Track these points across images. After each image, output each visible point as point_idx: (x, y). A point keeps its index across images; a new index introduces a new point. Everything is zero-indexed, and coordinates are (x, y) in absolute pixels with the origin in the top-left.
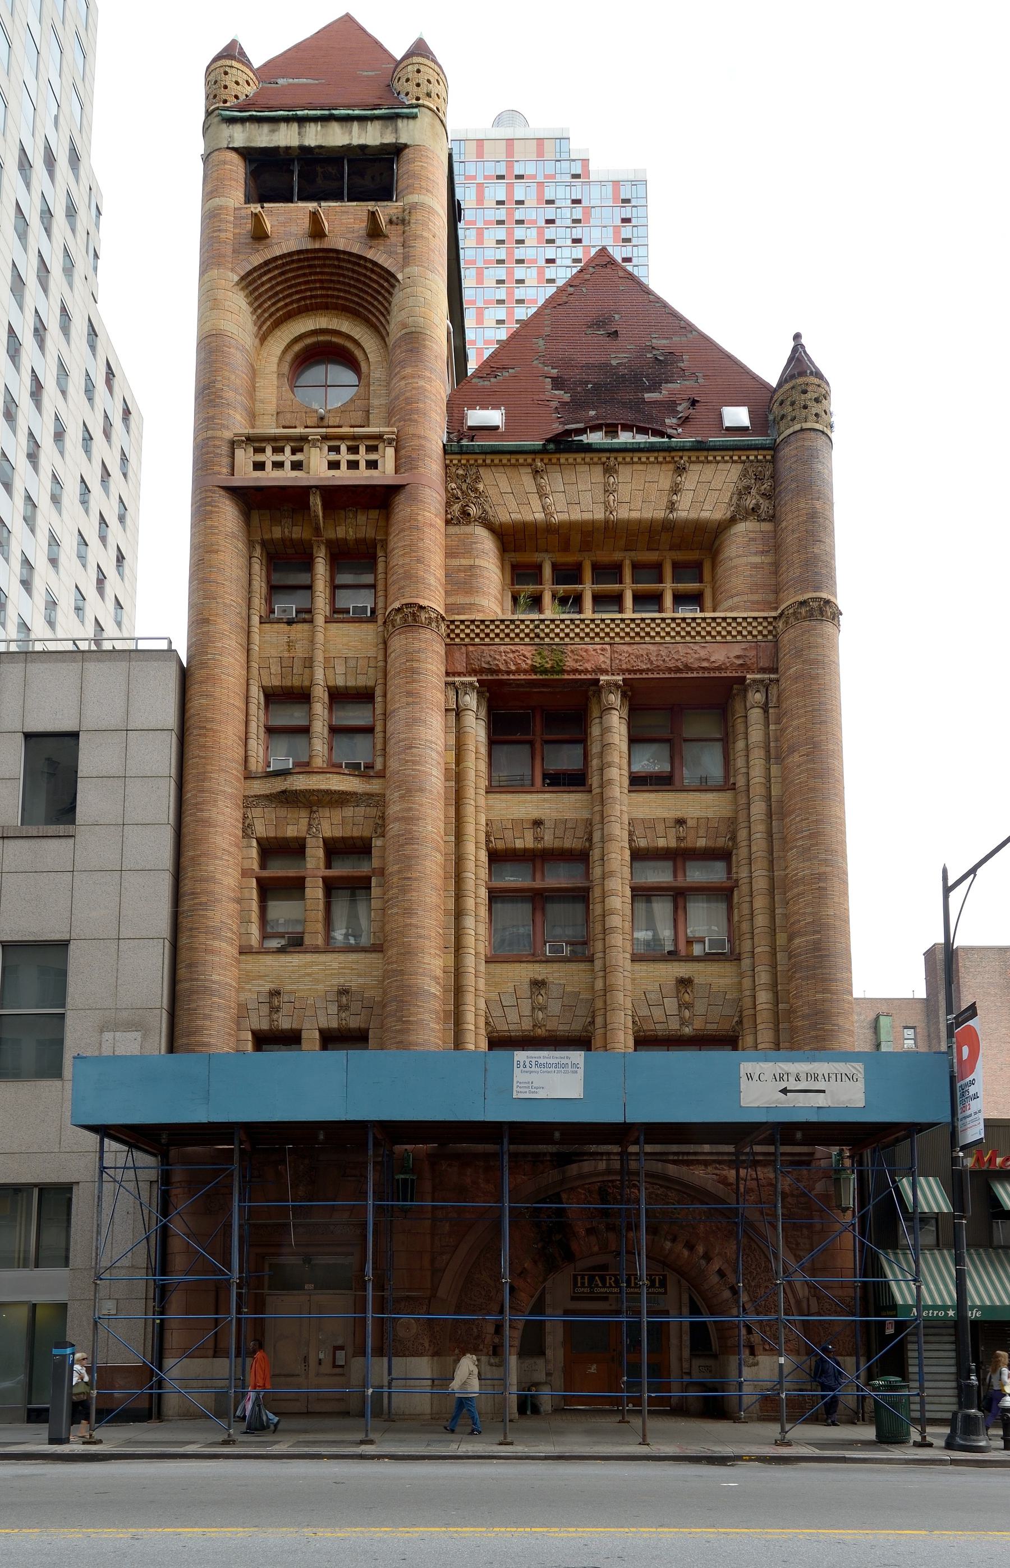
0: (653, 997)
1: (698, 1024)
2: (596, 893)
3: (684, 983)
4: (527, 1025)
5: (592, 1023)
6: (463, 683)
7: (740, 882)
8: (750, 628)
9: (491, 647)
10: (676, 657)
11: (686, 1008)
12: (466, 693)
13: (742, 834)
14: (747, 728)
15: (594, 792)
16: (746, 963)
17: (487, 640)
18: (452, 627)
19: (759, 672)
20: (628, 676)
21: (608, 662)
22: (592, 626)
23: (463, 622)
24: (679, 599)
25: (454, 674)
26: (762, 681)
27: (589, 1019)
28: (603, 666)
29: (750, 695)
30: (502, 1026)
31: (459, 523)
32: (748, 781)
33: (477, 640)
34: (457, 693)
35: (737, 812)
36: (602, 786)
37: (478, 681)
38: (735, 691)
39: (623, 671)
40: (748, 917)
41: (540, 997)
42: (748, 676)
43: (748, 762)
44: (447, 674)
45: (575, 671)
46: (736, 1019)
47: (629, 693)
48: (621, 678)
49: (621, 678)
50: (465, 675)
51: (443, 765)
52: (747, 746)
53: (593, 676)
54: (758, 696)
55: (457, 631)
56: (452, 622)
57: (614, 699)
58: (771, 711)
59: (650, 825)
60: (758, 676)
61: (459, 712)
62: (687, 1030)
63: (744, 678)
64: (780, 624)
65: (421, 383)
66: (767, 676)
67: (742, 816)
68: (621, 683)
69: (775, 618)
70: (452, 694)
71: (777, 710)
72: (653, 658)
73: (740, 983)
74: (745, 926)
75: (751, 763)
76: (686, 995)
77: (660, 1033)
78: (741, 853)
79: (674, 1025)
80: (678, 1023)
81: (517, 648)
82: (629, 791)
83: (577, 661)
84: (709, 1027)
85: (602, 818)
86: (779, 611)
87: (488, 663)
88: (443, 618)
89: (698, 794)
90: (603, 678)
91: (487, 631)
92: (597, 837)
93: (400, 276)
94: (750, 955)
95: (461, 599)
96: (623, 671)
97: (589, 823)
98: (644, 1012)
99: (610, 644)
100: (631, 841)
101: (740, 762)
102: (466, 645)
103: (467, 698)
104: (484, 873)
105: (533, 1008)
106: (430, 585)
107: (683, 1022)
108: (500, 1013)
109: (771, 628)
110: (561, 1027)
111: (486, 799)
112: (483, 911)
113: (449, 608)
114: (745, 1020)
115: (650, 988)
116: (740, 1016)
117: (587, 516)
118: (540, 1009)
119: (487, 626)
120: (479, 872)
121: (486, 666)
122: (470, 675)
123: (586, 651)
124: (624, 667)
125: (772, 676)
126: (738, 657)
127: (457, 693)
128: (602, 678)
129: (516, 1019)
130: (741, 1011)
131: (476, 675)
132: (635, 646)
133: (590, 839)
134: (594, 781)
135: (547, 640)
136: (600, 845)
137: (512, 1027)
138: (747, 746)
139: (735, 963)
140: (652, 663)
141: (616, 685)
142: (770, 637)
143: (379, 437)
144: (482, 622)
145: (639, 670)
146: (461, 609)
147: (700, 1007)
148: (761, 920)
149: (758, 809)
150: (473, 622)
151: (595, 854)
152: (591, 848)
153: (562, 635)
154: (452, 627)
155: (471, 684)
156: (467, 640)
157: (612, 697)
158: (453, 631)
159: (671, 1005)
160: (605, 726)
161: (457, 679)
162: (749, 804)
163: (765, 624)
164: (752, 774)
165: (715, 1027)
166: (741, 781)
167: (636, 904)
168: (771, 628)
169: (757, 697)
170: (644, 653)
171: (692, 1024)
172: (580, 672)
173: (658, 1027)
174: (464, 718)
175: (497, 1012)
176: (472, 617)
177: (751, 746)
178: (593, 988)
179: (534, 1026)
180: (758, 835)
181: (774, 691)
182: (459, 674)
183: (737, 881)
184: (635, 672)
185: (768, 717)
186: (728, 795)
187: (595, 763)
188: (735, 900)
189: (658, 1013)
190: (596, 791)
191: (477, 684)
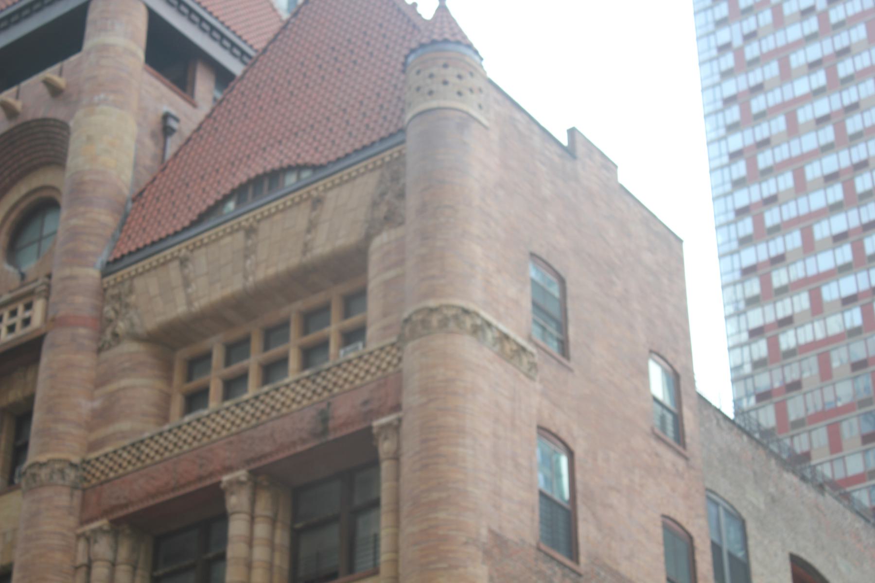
6: (94, 531)
20: (253, 466)
26: (389, 425)
31: (110, 347)
39: (248, 462)
45: (200, 478)
60: (383, 421)
61: (89, 567)
65: (74, 222)
70: (82, 545)
83: (201, 466)
90: (226, 478)
93: (71, 124)
95: (101, 433)
117: (228, 291)
126: (365, 403)
141: (239, 483)
143: (31, 293)
144: (115, 452)
150: (106, 455)
155: (100, 530)
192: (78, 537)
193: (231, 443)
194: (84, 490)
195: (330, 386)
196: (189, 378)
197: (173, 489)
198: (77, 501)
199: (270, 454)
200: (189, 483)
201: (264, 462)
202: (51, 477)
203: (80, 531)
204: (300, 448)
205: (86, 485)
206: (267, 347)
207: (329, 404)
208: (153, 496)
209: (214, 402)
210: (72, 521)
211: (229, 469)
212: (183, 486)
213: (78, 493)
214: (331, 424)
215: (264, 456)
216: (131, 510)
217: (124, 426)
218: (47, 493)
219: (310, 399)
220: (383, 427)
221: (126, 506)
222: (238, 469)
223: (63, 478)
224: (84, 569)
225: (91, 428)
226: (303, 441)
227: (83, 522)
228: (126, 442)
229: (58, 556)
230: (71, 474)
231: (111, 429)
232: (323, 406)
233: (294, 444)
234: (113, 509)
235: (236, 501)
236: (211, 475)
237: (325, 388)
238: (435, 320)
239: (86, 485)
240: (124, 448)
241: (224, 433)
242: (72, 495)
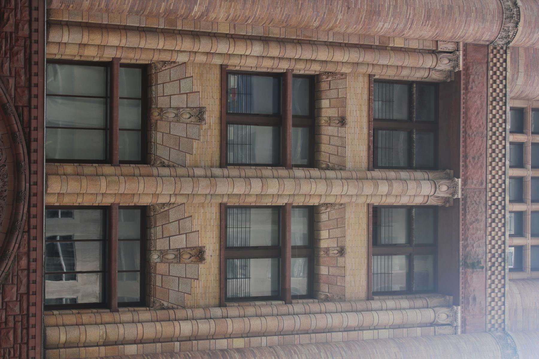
0: (187, 223)
1: (161, 268)
2: (282, 172)
3: (199, 255)
4: (162, 102)
5: (163, 165)
6: (458, 57)
7: (290, 306)
8: (496, 308)
9: (485, 84)
10: (475, 245)
11: (176, 256)
12: (450, 60)
13: (330, 306)
14: (418, 308)
15: (368, 173)
16: (218, 312)
17: (491, 81)
18: (501, 52)
19: (462, 317)
21: (473, 186)
22: (500, 173)
23: (505, 61)
24: (520, 249)
25: (465, 51)
26: (456, 320)
27: (166, 162)
28: (469, 181)
29: (445, 310)
30: (162, 77)
32: (375, 311)
33: (491, 73)
34: (450, 53)
35: (350, 301)
36: (372, 179)
37: (459, 72)
38: (448, 297)
40: (259, 312)
41: (188, 116)
42: (459, 307)
43: (391, 310)
44: (466, 45)
45: (466, 157)
46: (166, 304)
47: (448, 205)
48: (460, 197)
49: (460, 197)
50: (464, 60)
51: (392, 34)
52: (404, 309)
53: (461, 173)
54: (444, 316)
55: (498, 56)
56: (505, 52)
57: (443, 190)
58: (432, 328)
59: (340, 222)
60: (459, 315)
61: (435, 52)
62: (155, 257)
63: (457, 305)
64: (500, 334)
66: (459, 324)
67: (345, 306)
68: (456, 197)
69: (504, 329)
70: (450, 47)
71: (432, 333)
72: (474, 225)
73: (199, 307)
74: (250, 310)
75: (390, 313)
76: (188, 256)
77: (152, 231)
78: (314, 306)
79: (160, 244)
80: (162, 248)
81: (485, 107)
82: (368, 205)
83: (474, 158)
84: (158, 278)
85: (347, 179)
86: (509, 332)
87: (473, 81)
88: (509, 42)
89: (365, 267)
91: (498, 82)
92: (330, 174)
94: (225, 315)
95: (522, 62)
96: (465, 199)
97: (342, 167)
98: (173, 215)
99: (486, 188)
100: (326, 205)
101: (391, 303)
102: (487, 63)
103: (446, 61)
104: (301, 69)
105: (178, 109)
106: (534, 33)
107: (163, 253)
108: (174, 76)
109: (496, 326)
110: (159, 135)
111: (364, 75)
112: (266, 65)
113: (516, 49)
114: (164, 312)
115: (195, 222)
116: (168, 308)
118: (176, 115)
119: (501, 82)
120: (301, 63)
121: (471, 80)
122: (464, 65)
123: (481, 167)
124: (468, 200)
125: (459, 330)
126: (474, 299)
127: (450, 53)
128: (460, 180)
129: (167, 92)
130: (173, 308)
131: (464, 69)
132: (484, 209)
133: (328, 168)
134: (377, 173)
135: (490, 133)
136: (323, 175)
137: (160, 87)
138: (404, 309)
139: (217, 301)
140: (471, 224)
141: (455, 192)
142: (489, 326)
144: (505, 78)
145: (465, 212)
146: (515, 61)
147: (176, 269)
148: (256, 324)
149: (352, 320)
150: (505, 69)
151: (315, 172)
152: (320, 168)
153: (494, 146)
154: (501, 52)
155: (458, 65)
156: (491, 64)
157: (444, 188)
158: (498, 52)
159: (179, 242)
160: (422, 182)
161: (461, 52)
162: (356, 311)
163: (499, 321)
164: (381, 313)
165: (159, 283)
166: (375, 304)
167: (269, 211)
168: (496, 326)
169: (443, 315)
170: (479, 217)
171: (162, 262)
172: (465, 161)
173: (159, 229)
174: (431, 57)
175: (175, 73)
176: (509, 70)
177: (404, 312)
178: (197, 167)
179: (161, 109)
180: (330, 319)
181: (448, 330)
182: (465, 55)
183: (291, 303)
184: (464, 210)
185: (427, 326)
186: (363, 294)
187: (392, 174)
188: (274, 302)
189: (172, 228)
190: (369, 174)
191: (457, 70)
192: (457, 43)
193: (482, 184)
194: (488, 45)
195: (493, 269)
196: (533, 110)
197: (465, 132)
198: (482, 43)
199: (464, 220)
200: (465, 147)
201: (461, 212)
202: (505, 30)
203: (461, 45)
204: (461, 243)
205: (491, 47)
206: (532, 178)
207: (482, 268)
208: (466, 113)
209: (511, 138)
210: (470, 41)
211: (465, 183)
212: (465, 141)
213: (488, 43)
214: (470, 270)
215: (465, 215)
216: (462, 92)
217: (520, 81)
218: (495, 28)
219: (490, 252)
220: (456, 313)
221: (466, 88)
222: (463, 190)
223: (502, 38)
224: (434, 49)
225: (527, 49)
226: (465, 247)
227: (466, 45)
228: (509, 75)
229: (450, 35)
230: (501, 42)
231: (522, 68)
232: (483, 264)
233: (466, 239)
234: (467, 75)
235: (443, 190)
236: (466, 166)
237: (493, 265)
238: (510, 351)
239: (491, 47)
240: (505, 87)
241: (490, 177)
242: (488, 41)
